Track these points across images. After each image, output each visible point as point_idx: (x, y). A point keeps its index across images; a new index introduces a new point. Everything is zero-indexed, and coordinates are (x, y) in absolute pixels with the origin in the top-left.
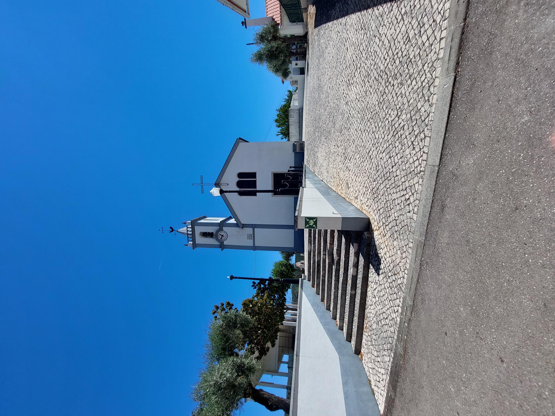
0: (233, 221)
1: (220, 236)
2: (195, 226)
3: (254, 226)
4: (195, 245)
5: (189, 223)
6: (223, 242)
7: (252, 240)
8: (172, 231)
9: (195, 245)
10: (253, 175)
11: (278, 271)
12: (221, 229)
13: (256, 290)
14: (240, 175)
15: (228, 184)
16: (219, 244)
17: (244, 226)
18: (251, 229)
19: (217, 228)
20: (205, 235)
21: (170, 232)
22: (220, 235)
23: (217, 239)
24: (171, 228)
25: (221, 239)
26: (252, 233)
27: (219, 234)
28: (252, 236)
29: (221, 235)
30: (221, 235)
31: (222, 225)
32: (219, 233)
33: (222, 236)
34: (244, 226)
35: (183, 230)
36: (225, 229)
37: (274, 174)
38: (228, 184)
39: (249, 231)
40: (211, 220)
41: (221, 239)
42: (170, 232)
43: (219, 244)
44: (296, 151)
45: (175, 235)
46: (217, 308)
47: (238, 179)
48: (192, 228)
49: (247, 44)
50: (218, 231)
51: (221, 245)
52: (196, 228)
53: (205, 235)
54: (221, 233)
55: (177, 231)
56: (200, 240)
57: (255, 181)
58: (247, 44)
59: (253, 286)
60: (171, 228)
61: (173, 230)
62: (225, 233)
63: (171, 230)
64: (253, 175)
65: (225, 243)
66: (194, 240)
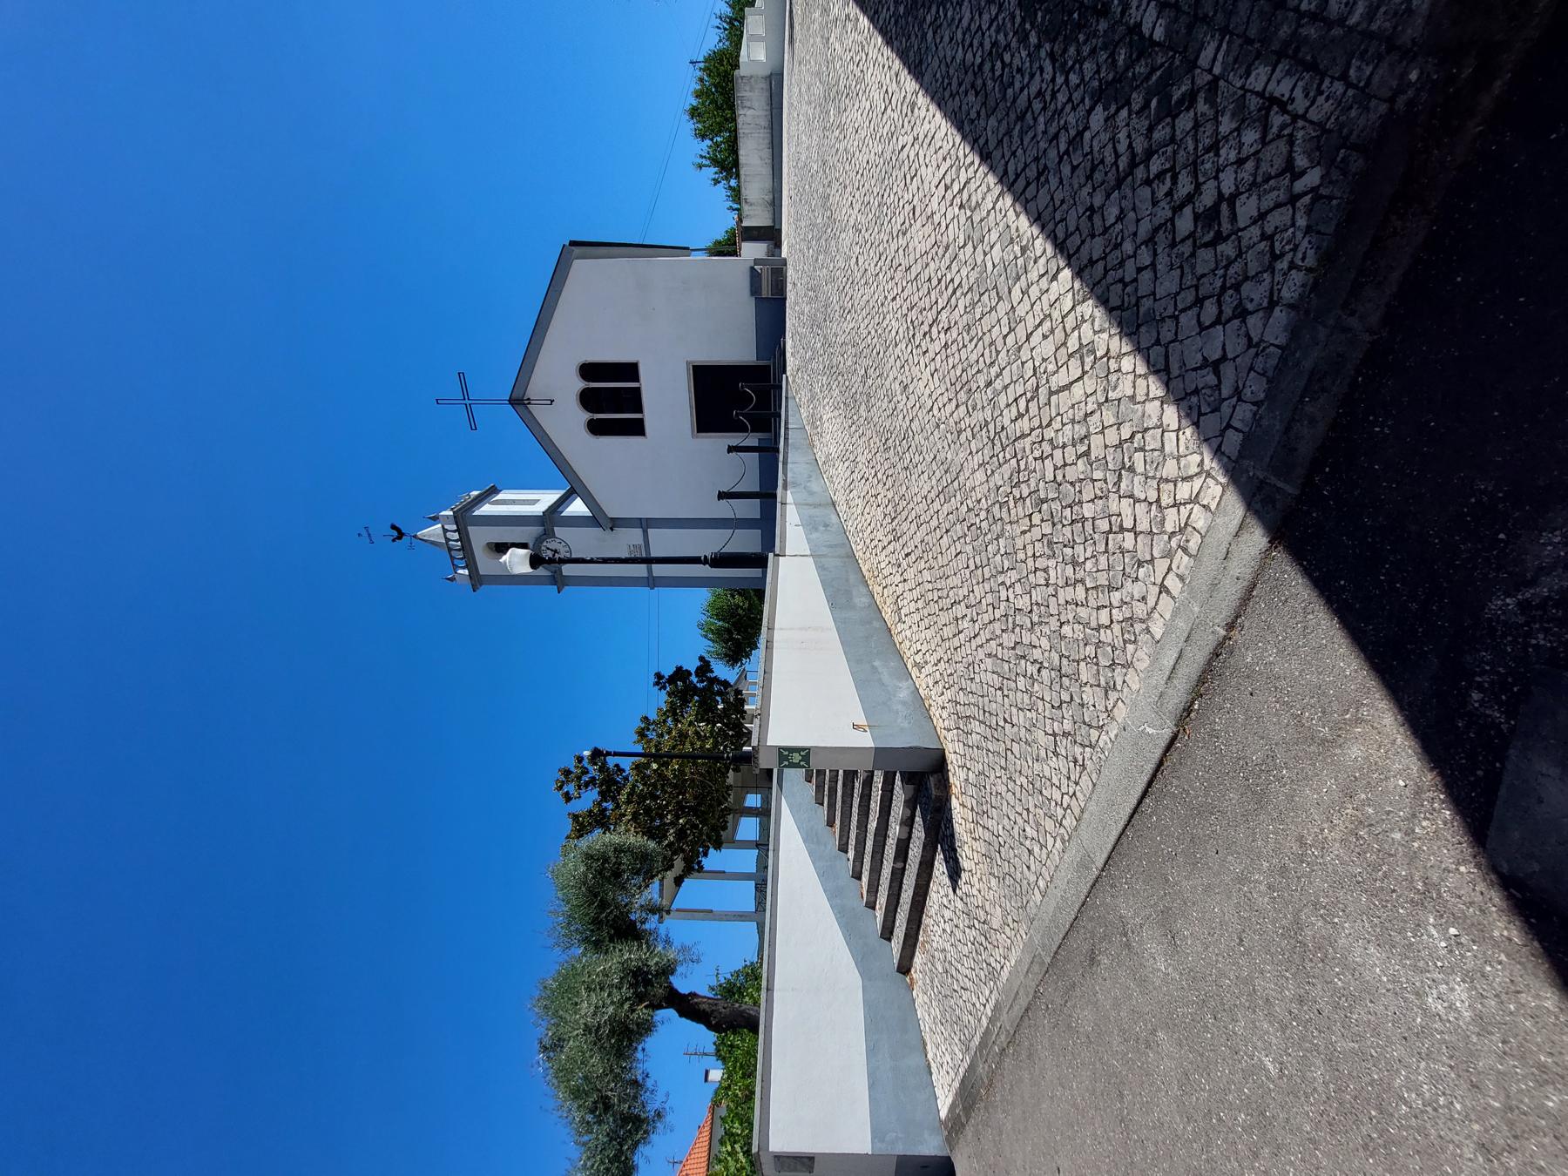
0: (577, 507)
4: (477, 580)
5: (447, 516)
9: (477, 580)
11: (721, 608)
13: (664, 692)
14: (589, 371)
15: (552, 401)
16: (549, 574)
17: (615, 523)
18: (639, 531)
19: (536, 530)
21: (394, 540)
24: (394, 527)
26: (641, 542)
31: (552, 517)
32: (545, 544)
34: (615, 523)
37: (694, 366)
38: (552, 401)
40: (513, 502)
42: (394, 540)
43: (549, 574)
44: (761, 294)
45: (411, 547)
46: (567, 773)
47: (581, 385)
48: (457, 530)
51: (553, 576)
52: (472, 531)
54: (549, 545)
55: (415, 537)
57: (638, 390)
59: (657, 684)
60: (394, 527)
61: (401, 535)
63: (395, 533)
66: (471, 564)
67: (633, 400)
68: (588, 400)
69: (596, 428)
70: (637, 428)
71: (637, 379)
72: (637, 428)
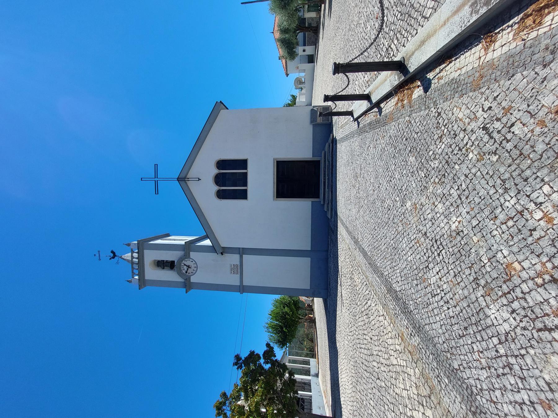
0: (207, 242)
1: (185, 268)
2: (145, 251)
3: (242, 252)
4: (143, 282)
5: (135, 244)
6: (190, 278)
7: (238, 275)
8: (113, 258)
9: (143, 282)
10: (243, 164)
11: (277, 313)
12: (187, 256)
13: (240, 371)
14: (221, 164)
15: (199, 179)
16: (182, 280)
17: (224, 251)
19: (179, 254)
20: (161, 264)
21: (110, 259)
22: (185, 265)
23: (180, 273)
24: (112, 252)
25: (186, 272)
26: (238, 263)
27: (183, 264)
28: (239, 268)
29: (187, 266)
30: (187, 266)
31: (189, 247)
32: (184, 262)
33: (189, 267)
34: (224, 251)
35: (128, 256)
36: (193, 255)
38: (199, 179)
39: (234, 259)
40: (175, 240)
41: (186, 272)
42: (110, 259)
43: (182, 280)
44: (316, 121)
45: (118, 263)
47: (216, 171)
48: (138, 253)
49: (242, 3)
50: (181, 259)
51: (185, 282)
52: (147, 252)
53: (161, 264)
54: (186, 263)
55: (121, 257)
56: (152, 273)
57: (246, 174)
58: (242, 3)
59: (235, 364)
60: (112, 252)
61: (114, 255)
62: (194, 262)
63: (112, 255)
64: (243, 164)
65: (193, 279)
66: (141, 274)
67: (243, 180)
68: (219, 180)
69: (221, 195)
70: (243, 195)
72: (243, 195)
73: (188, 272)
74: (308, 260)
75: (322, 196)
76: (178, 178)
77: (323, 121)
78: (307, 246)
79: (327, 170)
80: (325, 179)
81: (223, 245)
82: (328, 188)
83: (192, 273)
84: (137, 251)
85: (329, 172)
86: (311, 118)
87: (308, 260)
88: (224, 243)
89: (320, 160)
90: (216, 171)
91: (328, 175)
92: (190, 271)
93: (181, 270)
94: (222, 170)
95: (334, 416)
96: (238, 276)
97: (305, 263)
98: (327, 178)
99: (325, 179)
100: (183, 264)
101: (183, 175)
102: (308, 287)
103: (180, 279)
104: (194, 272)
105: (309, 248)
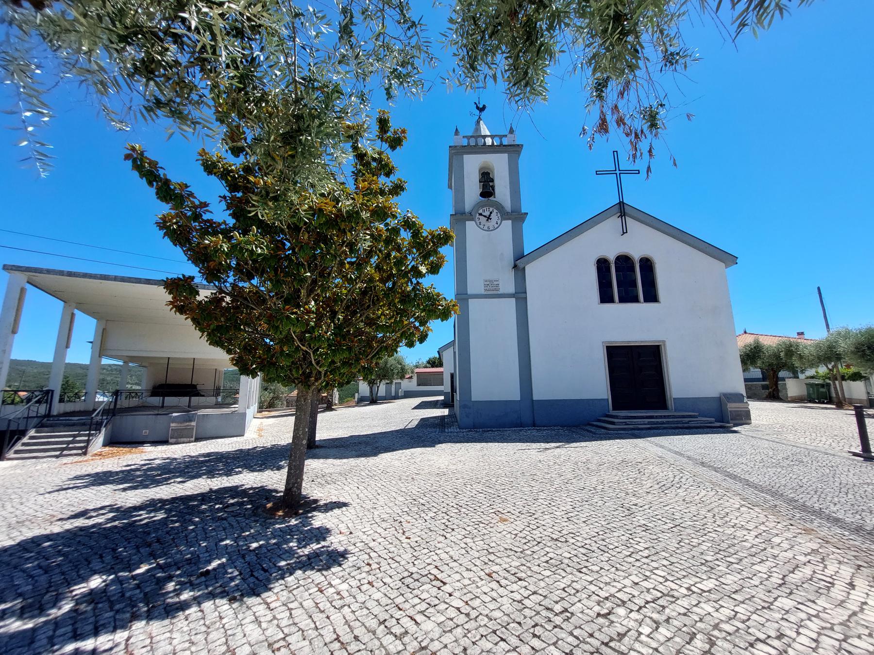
1: (487, 213)
2: (506, 155)
3: (520, 296)
6: (473, 220)
7: (483, 292)
8: (478, 108)
10: (652, 296)
12: (505, 215)
14: (647, 265)
18: (511, 289)
19: (508, 205)
20: (486, 179)
21: (475, 103)
22: (491, 213)
23: (479, 205)
25: (481, 214)
26: (501, 291)
27: (491, 209)
28: (495, 292)
29: (490, 216)
30: (490, 216)
32: (495, 211)
33: (489, 218)
36: (508, 224)
37: (658, 347)
39: (508, 285)
41: (481, 214)
42: (475, 103)
45: (471, 114)
46: (395, 143)
49: (819, 289)
50: (500, 207)
52: (504, 157)
53: (486, 179)
56: (473, 164)
57: (635, 300)
58: (819, 289)
62: (496, 226)
63: (481, 106)
64: (652, 296)
65: (470, 225)
67: (629, 297)
68: (624, 261)
69: (602, 265)
70: (606, 297)
71: (622, 300)
72: (606, 297)
73: (480, 217)
74: (516, 396)
75: (616, 413)
76: (623, 203)
77: (730, 411)
78: (539, 394)
79: (671, 420)
80: (657, 417)
81: (529, 269)
82: (649, 423)
83: (480, 223)
84: (495, 144)
85: (673, 423)
86: (731, 394)
87: (516, 396)
88: (531, 270)
89: (670, 407)
90: (612, 257)
91: (668, 423)
92: (483, 220)
93: (483, 207)
94: (640, 266)
95: (317, 444)
96: (482, 291)
97: (511, 392)
98: (664, 420)
99: (657, 417)
100: (491, 209)
101: (627, 209)
102: (474, 398)
103: (468, 205)
104: (482, 226)
105: (474, 398)
